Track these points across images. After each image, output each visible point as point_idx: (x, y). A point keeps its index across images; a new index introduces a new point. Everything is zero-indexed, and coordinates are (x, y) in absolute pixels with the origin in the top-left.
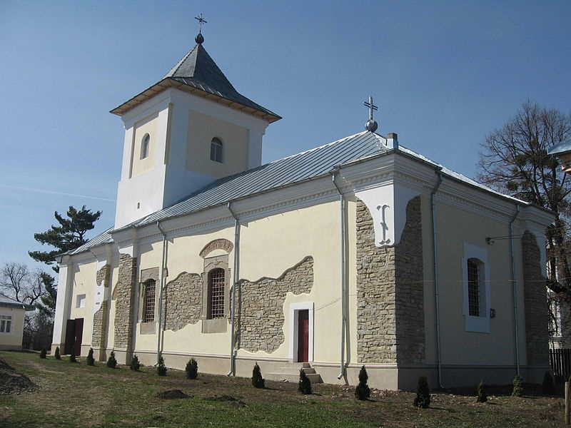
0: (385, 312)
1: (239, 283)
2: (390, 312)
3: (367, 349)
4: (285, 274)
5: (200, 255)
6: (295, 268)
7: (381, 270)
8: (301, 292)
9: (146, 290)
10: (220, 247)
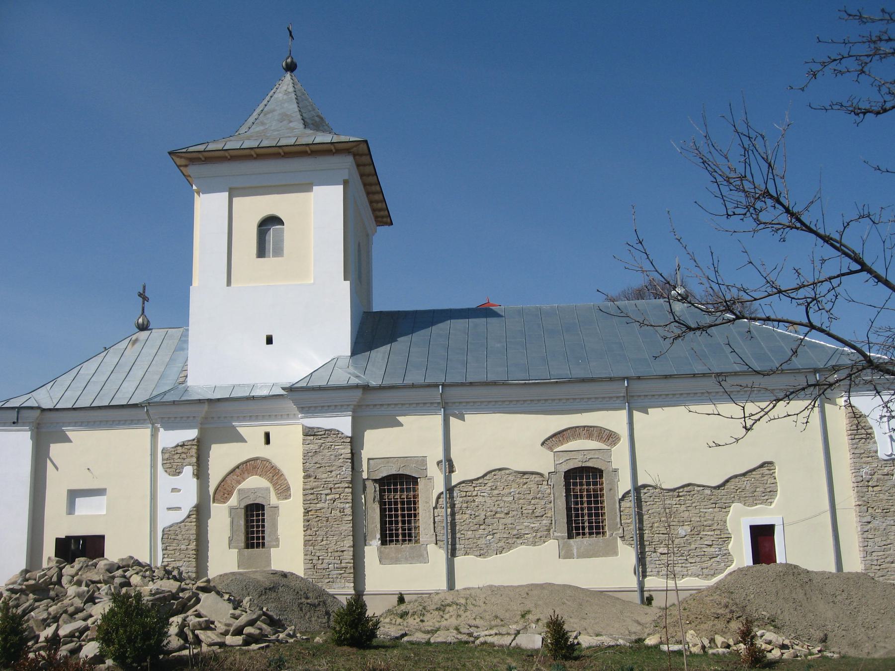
1: (638, 489)
3: (878, 567)
4: (727, 481)
5: (543, 444)
6: (744, 475)
7: (889, 483)
8: (756, 504)
9: (382, 491)
10: (590, 436)
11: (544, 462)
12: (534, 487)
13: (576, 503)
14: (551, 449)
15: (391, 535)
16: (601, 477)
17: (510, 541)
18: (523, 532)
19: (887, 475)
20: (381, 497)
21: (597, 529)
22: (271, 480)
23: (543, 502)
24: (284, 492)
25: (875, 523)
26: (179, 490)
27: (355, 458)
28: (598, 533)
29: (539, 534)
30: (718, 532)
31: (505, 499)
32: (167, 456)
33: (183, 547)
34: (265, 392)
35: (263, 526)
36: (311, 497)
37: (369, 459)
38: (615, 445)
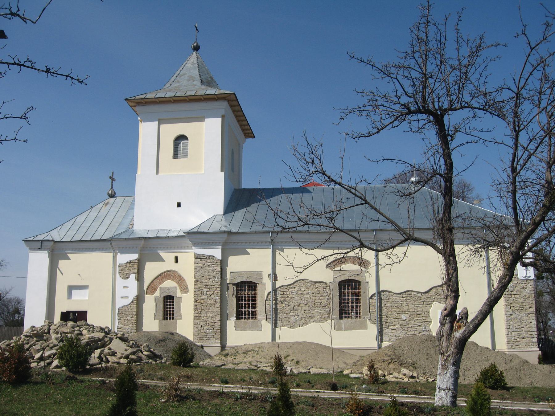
0: (527, 318)
1: (379, 293)
2: (532, 318)
4: (431, 289)
7: (524, 293)
9: (237, 290)
10: (353, 263)
11: (327, 276)
12: (321, 290)
15: (242, 315)
16: (360, 285)
17: (307, 319)
18: (314, 315)
19: (523, 288)
20: (237, 293)
22: (178, 283)
23: (326, 298)
24: (185, 289)
25: (515, 315)
26: (128, 287)
27: (223, 272)
29: (323, 317)
30: (425, 318)
31: (305, 296)
32: (121, 268)
33: (129, 318)
34: (175, 234)
35: (173, 308)
36: (198, 292)
37: (231, 272)
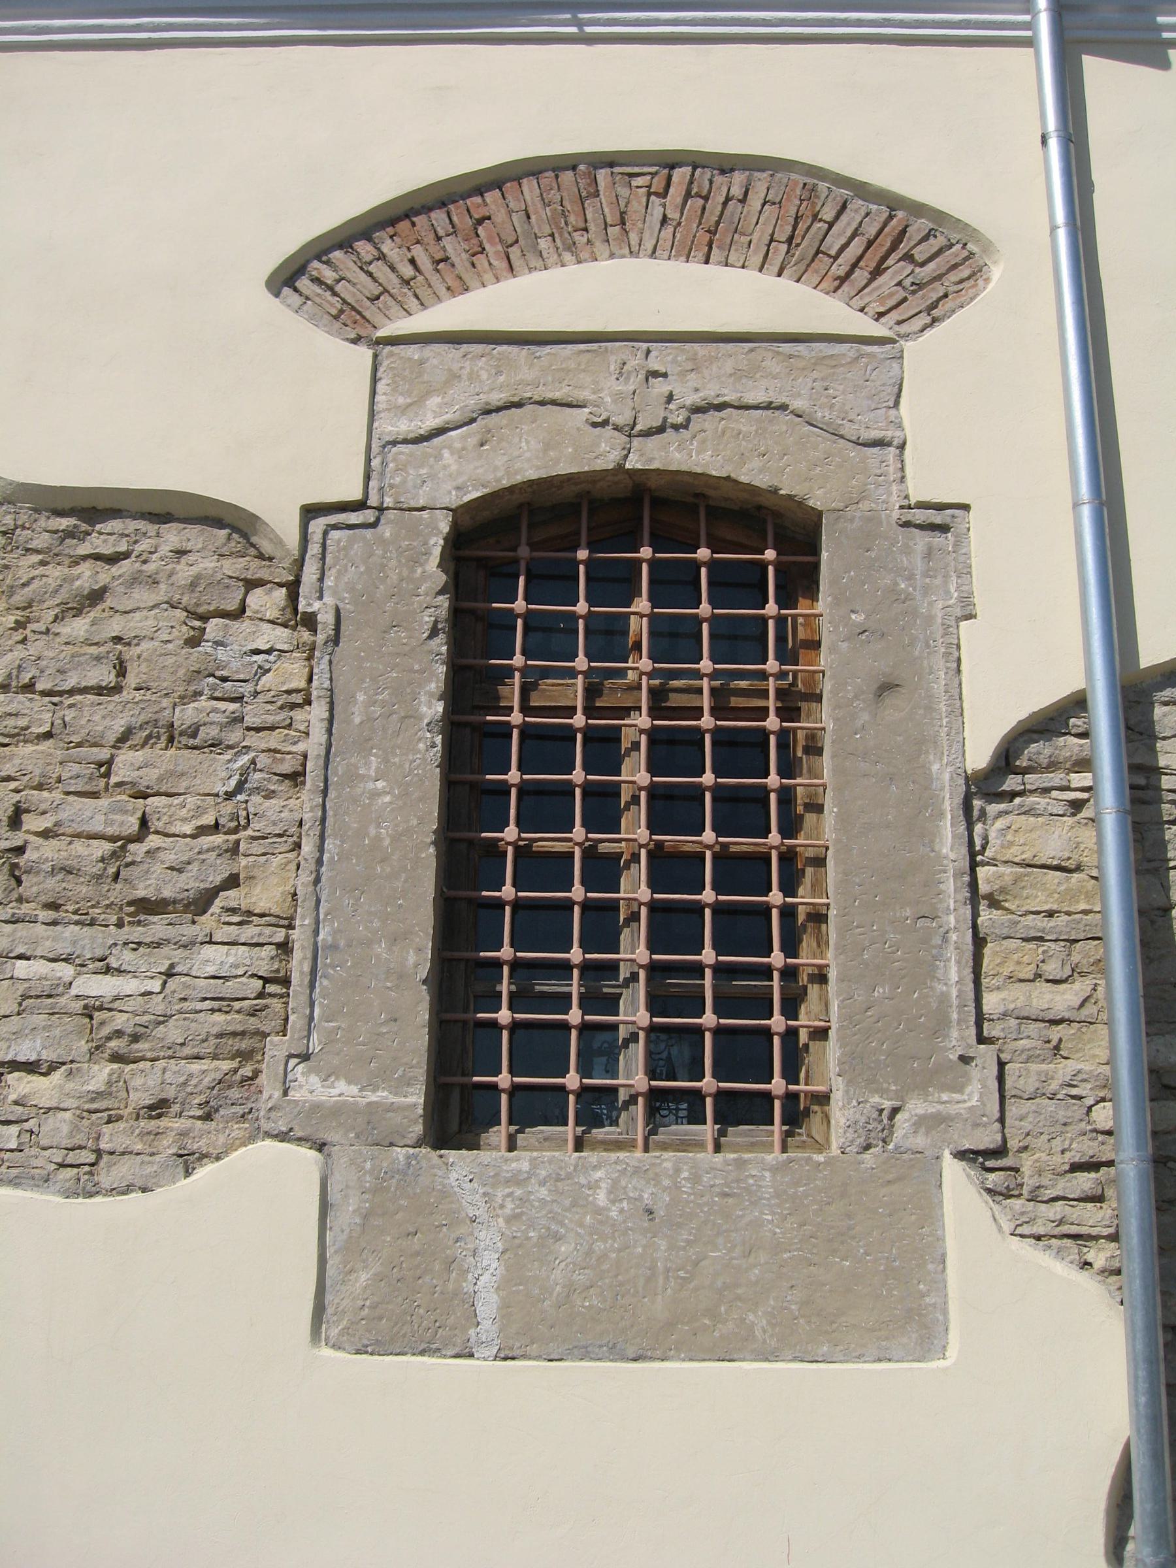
5: (287, 278)
10: (710, 241)
11: (285, 425)
12: (146, 622)
13: (547, 808)
14: (351, 321)
16: (801, 580)
21: (738, 1067)
23: (219, 772)
28: (741, 1111)
29: (145, 1083)
38: (933, 315)
